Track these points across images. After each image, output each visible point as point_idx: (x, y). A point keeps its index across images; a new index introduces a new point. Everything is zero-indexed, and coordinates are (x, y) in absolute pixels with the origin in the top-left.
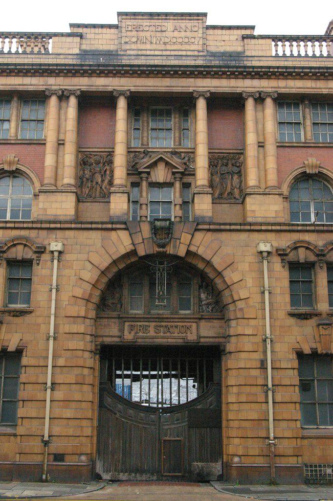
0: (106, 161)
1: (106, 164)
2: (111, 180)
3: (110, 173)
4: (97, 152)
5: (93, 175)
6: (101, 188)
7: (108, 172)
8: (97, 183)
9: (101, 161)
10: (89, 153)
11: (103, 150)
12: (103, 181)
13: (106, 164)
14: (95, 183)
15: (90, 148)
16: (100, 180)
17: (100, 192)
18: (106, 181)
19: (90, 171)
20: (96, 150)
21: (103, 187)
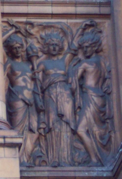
0: (80, 47)
1: (80, 56)
2: (104, 105)
3: (97, 83)
4: (53, 15)
5: (43, 92)
6: (74, 132)
7: (90, 81)
8: (61, 116)
9: (66, 48)
10: (24, 19)
11: (71, 10)
12: (77, 110)
13: (80, 56)
14: (53, 116)
15: (27, 4)
16: (67, 108)
17: (74, 148)
18: (90, 112)
19: (34, 79)
20: (48, 9)
21: (81, 131)
